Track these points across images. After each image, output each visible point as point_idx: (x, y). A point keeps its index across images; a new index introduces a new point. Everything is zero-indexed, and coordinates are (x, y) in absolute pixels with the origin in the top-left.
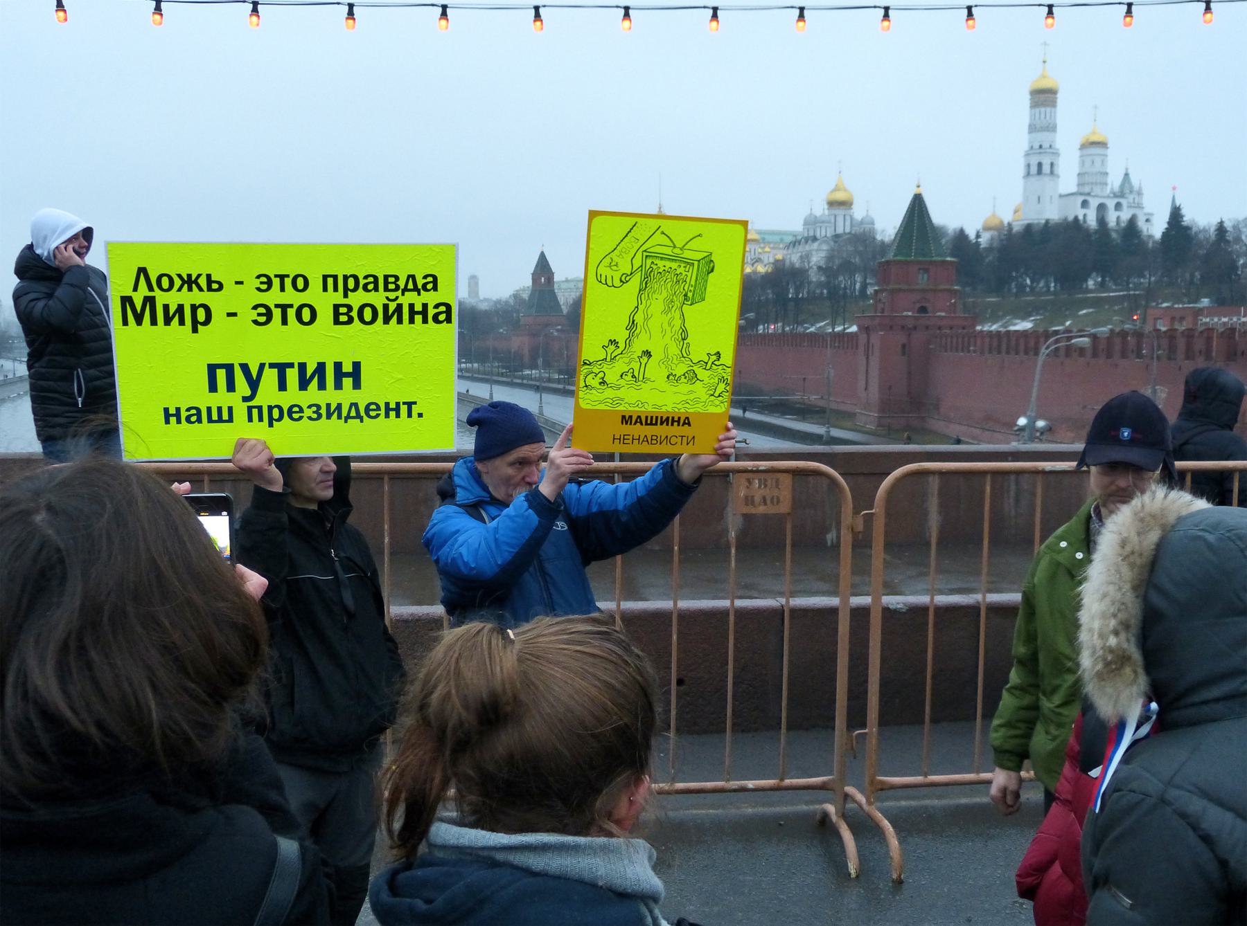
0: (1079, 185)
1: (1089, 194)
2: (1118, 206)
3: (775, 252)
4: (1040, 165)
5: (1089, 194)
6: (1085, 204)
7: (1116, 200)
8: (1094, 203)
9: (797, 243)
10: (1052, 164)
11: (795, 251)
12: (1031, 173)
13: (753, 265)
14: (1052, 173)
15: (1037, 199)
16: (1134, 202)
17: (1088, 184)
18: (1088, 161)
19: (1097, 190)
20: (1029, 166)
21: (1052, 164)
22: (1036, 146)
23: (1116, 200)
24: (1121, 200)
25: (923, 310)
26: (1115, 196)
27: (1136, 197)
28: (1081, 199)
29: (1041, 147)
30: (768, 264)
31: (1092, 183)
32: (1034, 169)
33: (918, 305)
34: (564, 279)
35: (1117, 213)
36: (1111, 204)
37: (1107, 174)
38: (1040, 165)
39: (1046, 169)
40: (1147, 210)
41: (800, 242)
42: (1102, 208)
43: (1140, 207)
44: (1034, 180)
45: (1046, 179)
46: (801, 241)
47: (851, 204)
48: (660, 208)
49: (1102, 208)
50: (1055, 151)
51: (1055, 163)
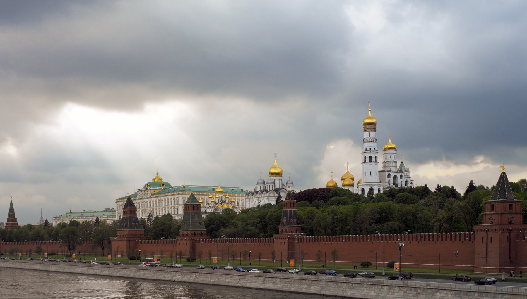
0: (384, 167)
1: (390, 171)
2: (401, 176)
3: (230, 197)
4: (371, 157)
5: (390, 171)
6: (389, 175)
7: (400, 174)
8: (392, 175)
9: (255, 193)
10: (376, 157)
11: (253, 197)
12: (366, 161)
13: (221, 204)
14: (376, 161)
15: (370, 173)
16: (406, 175)
17: (389, 166)
18: (388, 156)
19: (393, 169)
20: (365, 158)
21: (376, 157)
22: (368, 149)
23: (400, 174)
24: (402, 174)
25: (511, 222)
26: (399, 173)
27: (407, 172)
28: (388, 173)
29: (370, 149)
30: (228, 203)
31: (391, 166)
32: (368, 160)
33: (509, 221)
34: (83, 211)
35: (401, 180)
36: (398, 175)
37: (397, 162)
38: (371, 157)
39: (373, 160)
40: (411, 179)
41: (257, 193)
42: (395, 177)
43: (409, 177)
44: (367, 165)
45: (373, 164)
46: (258, 192)
47: (282, 174)
48: (157, 175)
49: (395, 177)
50: (377, 151)
51: (377, 157)
